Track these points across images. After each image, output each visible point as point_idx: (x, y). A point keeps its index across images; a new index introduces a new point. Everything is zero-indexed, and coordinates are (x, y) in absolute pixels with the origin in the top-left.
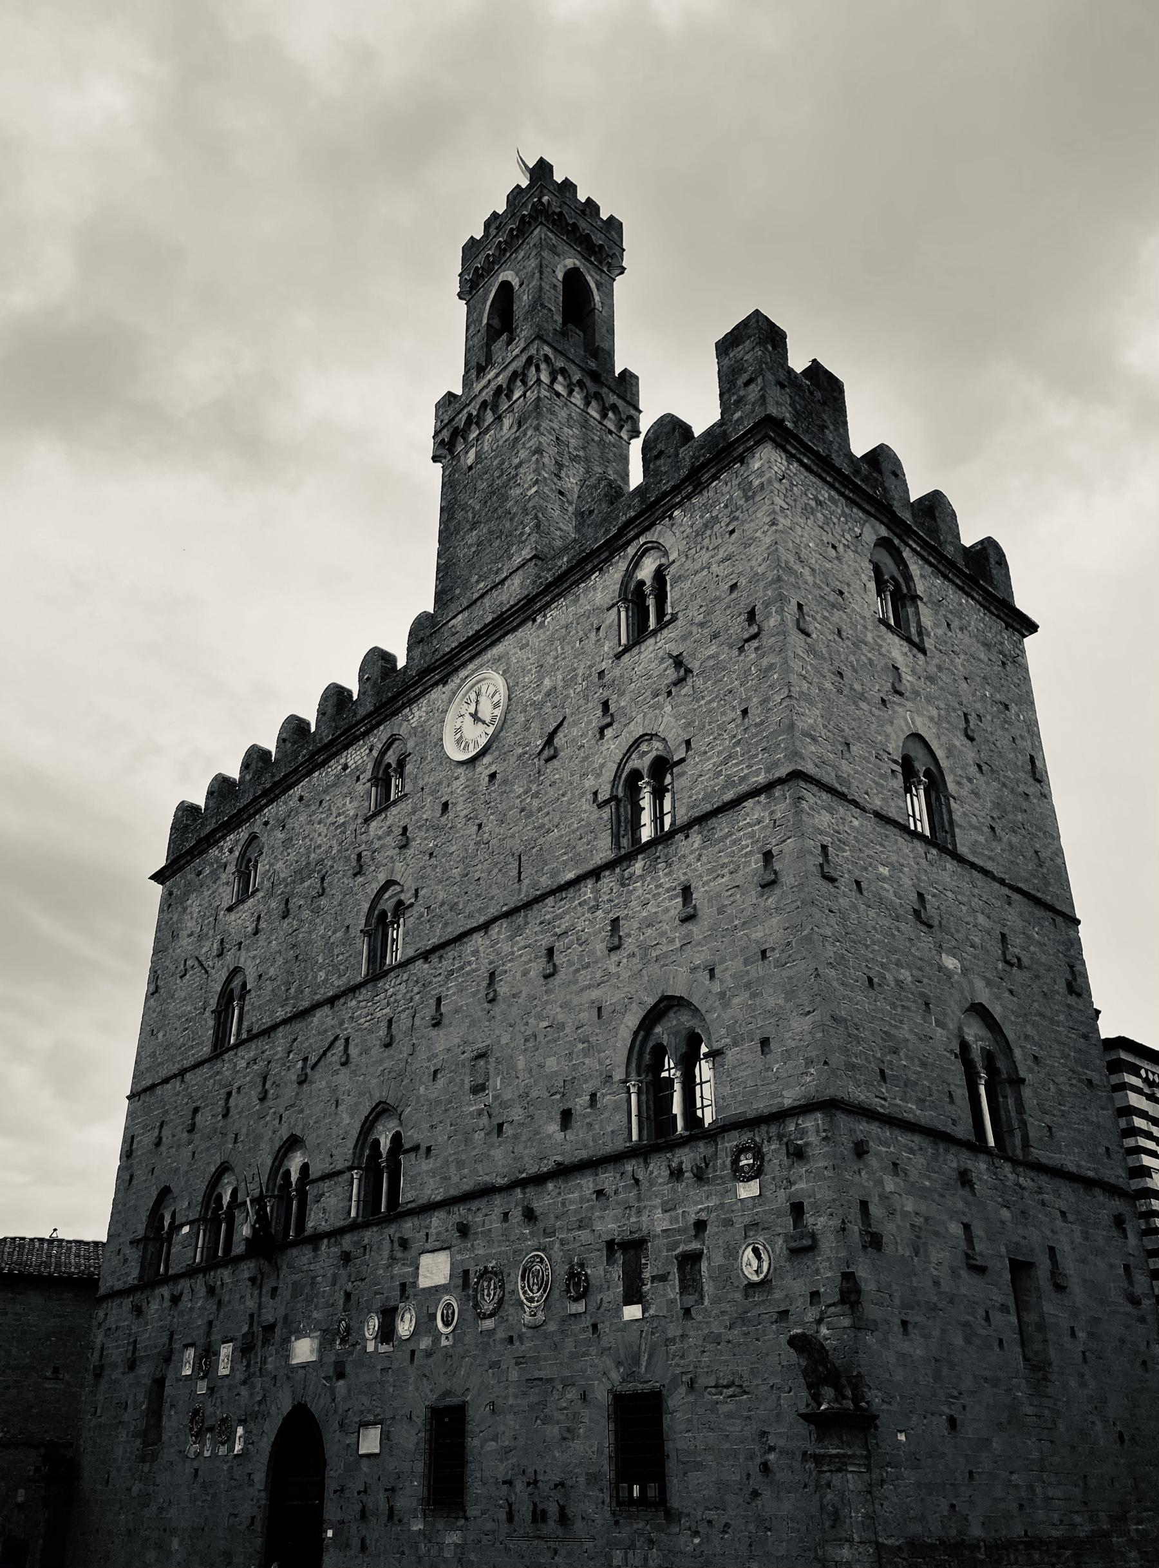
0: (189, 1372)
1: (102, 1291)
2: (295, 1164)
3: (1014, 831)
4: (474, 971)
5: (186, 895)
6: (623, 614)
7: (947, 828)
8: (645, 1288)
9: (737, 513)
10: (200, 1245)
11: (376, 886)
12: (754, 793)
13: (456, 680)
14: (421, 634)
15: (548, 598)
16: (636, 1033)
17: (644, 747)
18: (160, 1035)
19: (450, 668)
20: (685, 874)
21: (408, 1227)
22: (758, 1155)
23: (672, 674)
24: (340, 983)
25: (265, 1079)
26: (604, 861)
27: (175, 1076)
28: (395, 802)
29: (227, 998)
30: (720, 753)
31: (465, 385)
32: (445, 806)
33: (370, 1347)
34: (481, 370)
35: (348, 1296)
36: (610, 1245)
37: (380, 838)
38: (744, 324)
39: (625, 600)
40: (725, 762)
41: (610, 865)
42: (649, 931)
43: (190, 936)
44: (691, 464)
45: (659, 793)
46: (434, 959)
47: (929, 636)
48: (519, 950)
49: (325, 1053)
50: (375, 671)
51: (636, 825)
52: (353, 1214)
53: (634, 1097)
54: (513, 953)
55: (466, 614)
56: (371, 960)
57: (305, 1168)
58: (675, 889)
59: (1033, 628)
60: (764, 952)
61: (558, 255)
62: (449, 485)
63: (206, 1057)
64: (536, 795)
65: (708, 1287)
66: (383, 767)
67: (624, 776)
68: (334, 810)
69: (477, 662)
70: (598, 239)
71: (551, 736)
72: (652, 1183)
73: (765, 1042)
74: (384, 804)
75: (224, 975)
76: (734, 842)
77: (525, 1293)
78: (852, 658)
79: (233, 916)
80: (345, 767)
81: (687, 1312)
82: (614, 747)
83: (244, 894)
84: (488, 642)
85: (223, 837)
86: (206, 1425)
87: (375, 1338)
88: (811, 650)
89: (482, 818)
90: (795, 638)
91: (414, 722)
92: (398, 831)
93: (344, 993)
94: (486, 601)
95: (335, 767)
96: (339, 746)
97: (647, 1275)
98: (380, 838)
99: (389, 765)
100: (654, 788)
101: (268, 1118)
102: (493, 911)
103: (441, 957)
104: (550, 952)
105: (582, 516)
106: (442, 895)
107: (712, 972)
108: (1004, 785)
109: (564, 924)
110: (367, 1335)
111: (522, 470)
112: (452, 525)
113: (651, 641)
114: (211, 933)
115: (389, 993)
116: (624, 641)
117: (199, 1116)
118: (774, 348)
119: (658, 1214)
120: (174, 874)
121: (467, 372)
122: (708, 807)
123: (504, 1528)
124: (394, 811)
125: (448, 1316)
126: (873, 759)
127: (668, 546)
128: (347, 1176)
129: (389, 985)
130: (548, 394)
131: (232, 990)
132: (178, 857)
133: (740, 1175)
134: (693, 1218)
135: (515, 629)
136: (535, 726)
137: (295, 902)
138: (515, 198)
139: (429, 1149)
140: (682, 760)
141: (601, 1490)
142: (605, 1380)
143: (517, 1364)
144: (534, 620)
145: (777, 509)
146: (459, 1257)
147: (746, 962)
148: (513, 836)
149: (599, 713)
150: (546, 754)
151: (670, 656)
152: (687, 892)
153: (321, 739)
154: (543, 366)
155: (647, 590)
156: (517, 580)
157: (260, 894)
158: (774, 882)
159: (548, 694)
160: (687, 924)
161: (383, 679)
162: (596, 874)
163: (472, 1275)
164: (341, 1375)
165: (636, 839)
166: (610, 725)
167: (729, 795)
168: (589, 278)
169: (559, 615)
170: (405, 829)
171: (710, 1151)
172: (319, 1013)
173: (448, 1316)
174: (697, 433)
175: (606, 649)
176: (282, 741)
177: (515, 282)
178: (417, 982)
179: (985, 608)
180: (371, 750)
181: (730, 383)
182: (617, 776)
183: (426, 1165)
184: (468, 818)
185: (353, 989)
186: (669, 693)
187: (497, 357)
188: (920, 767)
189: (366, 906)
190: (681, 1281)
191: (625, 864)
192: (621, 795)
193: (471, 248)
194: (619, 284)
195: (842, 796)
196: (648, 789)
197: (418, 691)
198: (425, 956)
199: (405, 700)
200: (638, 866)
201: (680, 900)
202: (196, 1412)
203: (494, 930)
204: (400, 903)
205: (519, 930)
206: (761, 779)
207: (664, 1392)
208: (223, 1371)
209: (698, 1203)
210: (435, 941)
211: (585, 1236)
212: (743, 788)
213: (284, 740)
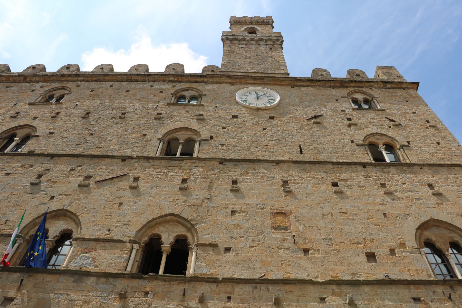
16: (417, 229)
21: (204, 288)
25: (40, 176)
80: (152, 86)
103: (236, 165)
115: (186, 167)
128: (129, 245)
129: (186, 164)
135: (281, 85)
139: (227, 250)
162: (364, 165)
183: (229, 256)
197: (215, 80)
201: (427, 187)
213: (102, 68)
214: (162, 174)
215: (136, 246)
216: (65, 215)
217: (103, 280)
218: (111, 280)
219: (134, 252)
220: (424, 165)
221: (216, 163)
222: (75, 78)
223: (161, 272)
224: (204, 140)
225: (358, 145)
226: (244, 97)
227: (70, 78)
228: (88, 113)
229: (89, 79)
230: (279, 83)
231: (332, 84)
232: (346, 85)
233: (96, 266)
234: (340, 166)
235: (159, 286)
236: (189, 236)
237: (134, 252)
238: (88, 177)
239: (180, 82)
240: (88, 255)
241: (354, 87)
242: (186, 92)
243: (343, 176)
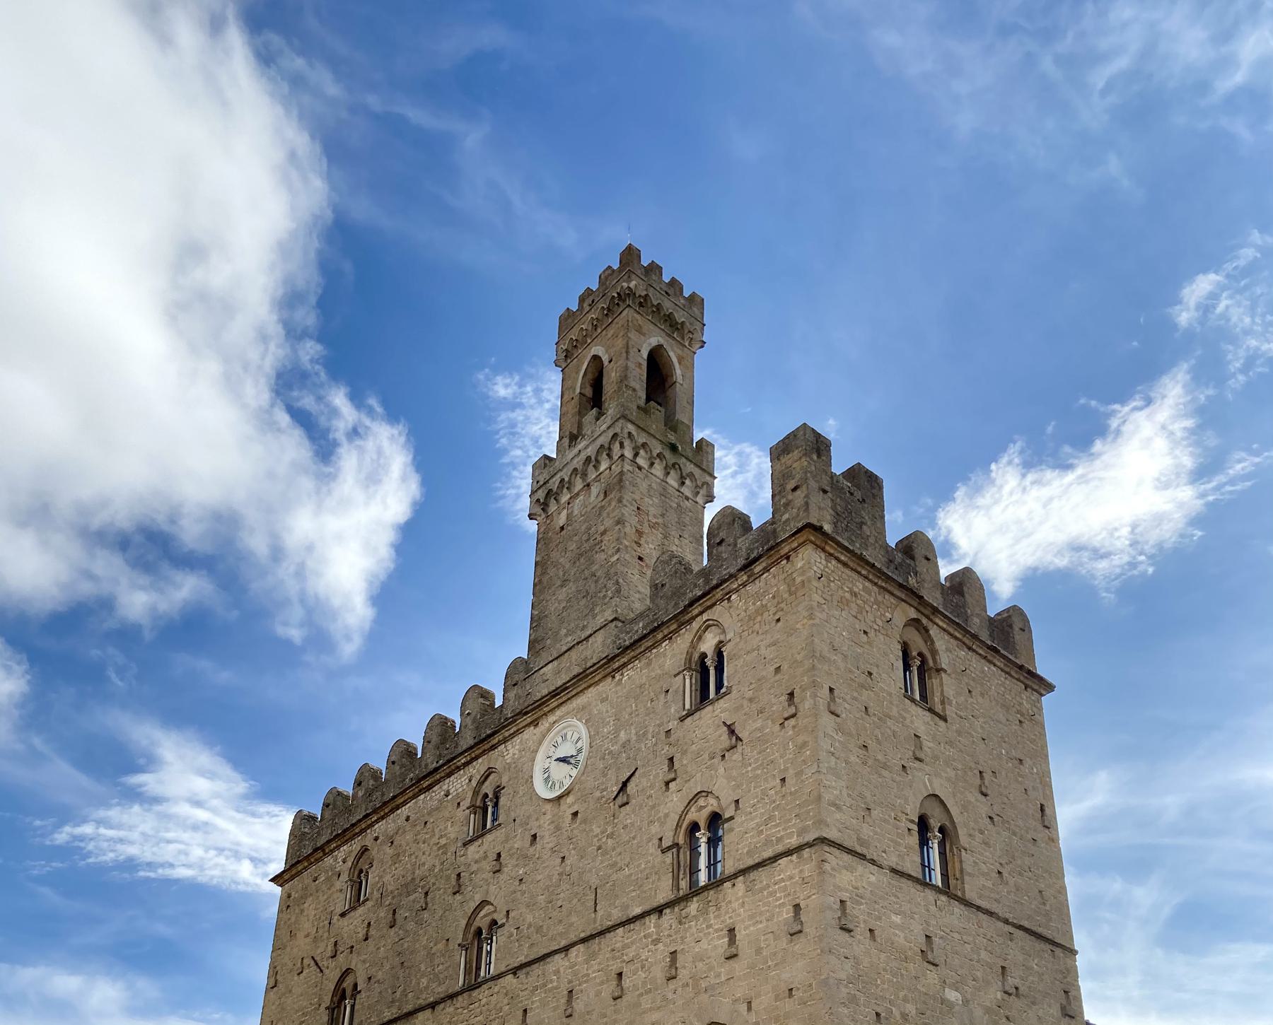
3: (1020, 874)
4: (556, 988)
5: (304, 898)
6: (688, 681)
7: (958, 875)
9: (782, 605)
11: (473, 905)
12: (788, 853)
13: (544, 724)
14: (516, 678)
15: (625, 660)
17: (701, 802)
19: (540, 713)
23: (725, 741)
24: (441, 990)
26: (666, 900)
28: (490, 830)
29: (340, 995)
30: (762, 814)
31: (558, 451)
32: (534, 836)
34: (574, 438)
37: (476, 862)
38: (792, 436)
39: (690, 669)
41: (670, 904)
42: (700, 965)
43: (307, 936)
44: (750, 551)
45: (713, 842)
46: (521, 974)
47: (950, 704)
50: (475, 706)
51: (694, 870)
54: (588, 975)
55: (555, 663)
56: (467, 972)
59: (1050, 687)
61: (644, 335)
62: (543, 541)
64: (611, 836)
68: (437, 831)
69: (564, 709)
70: (680, 317)
71: (625, 784)
74: (482, 831)
75: (337, 974)
78: (877, 732)
79: (345, 921)
82: (674, 801)
83: (357, 902)
85: (338, 847)
88: (839, 729)
89: (565, 852)
90: (827, 720)
91: (508, 759)
92: (493, 856)
93: (443, 1000)
94: (573, 653)
95: (438, 791)
98: (476, 862)
99: (486, 796)
100: (709, 839)
102: (573, 937)
105: (656, 588)
106: (529, 918)
108: (1014, 834)
109: (631, 953)
111: (606, 538)
112: (545, 579)
113: (710, 708)
114: (326, 935)
116: (688, 706)
118: (819, 456)
120: (292, 878)
121: (561, 438)
122: (750, 862)
124: (489, 838)
126: (892, 821)
127: (726, 626)
129: (482, 994)
130: (630, 468)
131: (344, 990)
132: (298, 862)
135: (596, 683)
136: (611, 774)
137: (402, 913)
138: (606, 278)
140: (732, 818)
144: (613, 677)
145: (815, 604)
148: (590, 871)
149: (666, 768)
150: (620, 800)
152: (732, 931)
153: (426, 765)
154: (627, 443)
155: (709, 662)
156: (599, 637)
157: (369, 904)
160: (731, 961)
161: (483, 715)
162: (659, 910)
165: (693, 882)
166: (674, 779)
167: (768, 853)
168: (671, 354)
169: (634, 675)
170: (499, 855)
172: (421, 1015)
174: (755, 524)
176: (391, 763)
177: (605, 359)
179: (1007, 673)
181: (781, 486)
182: (678, 826)
184: (553, 851)
185: (452, 997)
186: (723, 756)
187: (587, 430)
188: (935, 823)
189: (464, 922)
191: (682, 905)
192: (681, 841)
193: (567, 320)
194: (700, 358)
195: (862, 857)
196: (704, 839)
198: (515, 971)
199: (501, 738)
200: (693, 906)
204: (494, 922)
205: (593, 956)
206: (794, 841)
210: (522, 959)
212: (780, 848)
213: (393, 763)
231: (666, 632)
232: (687, 617)
239: (476, 758)
241: (701, 613)
242: (487, 783)
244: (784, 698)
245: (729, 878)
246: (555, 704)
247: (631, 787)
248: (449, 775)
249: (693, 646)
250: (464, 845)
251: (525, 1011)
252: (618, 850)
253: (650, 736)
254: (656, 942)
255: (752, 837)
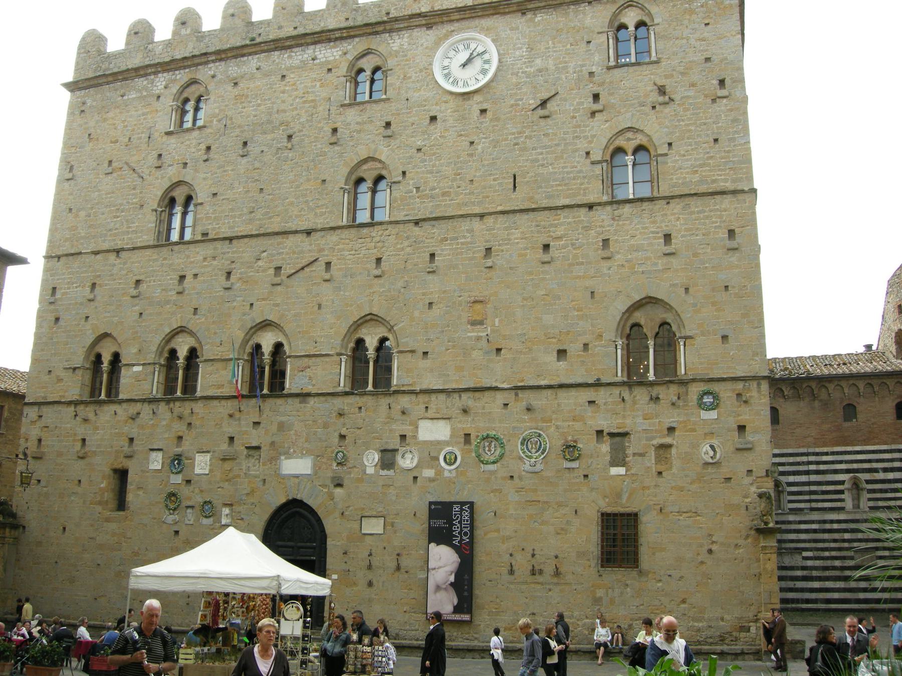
0: (159, 467)
1: (26, 400)
2: (267, 341)
6: (611, 41)
8: (627, 459)
10: (156, 380)
12: (723, 193)
16: (624, 314)
17: (630, 135)
18: (82, 214)
20: (667, 226)
21: (404, 401)
22: (716, 397)
25: (229, 274)
27: (108, 251)
33: (370, 471)
35: (342, 437)
36: (600, 433)
37: (357, 123)
40: (701, 166)
46: (426, 225)
48: (517, 239)
49: (303, 268)
52: (342, 384)
53: (619, 351)
57: (278, 346)
58: (658, 233)
60: (726, 287)
63: (151, 243)
64: (530, 137)
65: (676, 463)
66: (355, 69)
67: (612, 148)
72: (634, 403)
73: (725, 338)
76: (707, 217)
77: (524, 453)
79: (172, 140)
81: (660, 473)
84: (479, 14)
85: (155, 73)
86: (184, 504)
87: (376, 466)
96: (309, 41)
97: (629, 451)
98: (357, 123)
101: (235, 304)
104: (546, 247)
107: (687, 289)
110: (366, 463)
115: (378, 239)
117: (143, 287)
119: (640, 420)
123: (506, 577)
125: (450, 459)
128: (337, 358)
133: (701, 405)
134: (668, 425)
135: (505, 14)
139: (425, 353)
140: (666, 155)
141: (589, 560)
142: (594, 504)
143: (517, 492)
144: (524, 14)
146: (459, 426)
147: (713, 290)
151: (655, 84)
152: (667, 238)
158: (736, 249)
159: (540, 71)
162: (590, 207)
163: (473, 437)
164: (339, 485)
166: (601, 111)
167: (703, 189)
171: (682, 390)
173: (450, 459)
175: (596, 59)
178: (408, 238)
180: (345, 54)
186: (654, 107)
189: (345, 171)
190: (656, 458)
191: (615, 206)
197: (402, 26)
198: (416, 223)
199: (388, 27)
201: (662, 241)
202: (172, 494)
203: (490, 220)
206: (729, 186)
207: (641, 515)
208: (197, 471)
209: (672, 418)
211: (578, 425)
212: (713, 188)
214: (353, 252)
215: (344, 358)
216: (269, 325)
217: (322, 399)
218: (329, 398)
219: (343, 364)
220: (673, 197)
221: (411, 225)
222: (203, 59)
223: (370, 387)
224: (394, 182)
225: (593, 163)
226: (446, 62)
227: (197, 61)
228: (245, 144)
229: (223, 56)
230: (502, 11)
233: (314, 385)
234: (559, 212)
235: (368, 401)
236: (390, 336)
237: (343, 364)
238: (278, 269)
240: (304, 373)
242: (364, 60)
243: (559, 233)
244: (715, 82)
245: (669, 199)
246: (458, 17)
247: (548, 105)
248: (315, 43)
249: (615, 15)
250: (342, 106)
251: (432, 256)
252: (539, 150)
253: (571, 70)
254: (587, 228)
255: (688, 173)
